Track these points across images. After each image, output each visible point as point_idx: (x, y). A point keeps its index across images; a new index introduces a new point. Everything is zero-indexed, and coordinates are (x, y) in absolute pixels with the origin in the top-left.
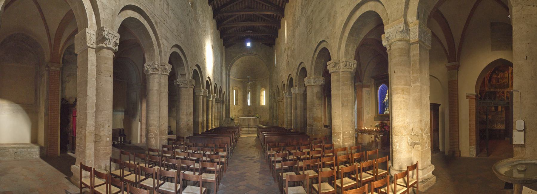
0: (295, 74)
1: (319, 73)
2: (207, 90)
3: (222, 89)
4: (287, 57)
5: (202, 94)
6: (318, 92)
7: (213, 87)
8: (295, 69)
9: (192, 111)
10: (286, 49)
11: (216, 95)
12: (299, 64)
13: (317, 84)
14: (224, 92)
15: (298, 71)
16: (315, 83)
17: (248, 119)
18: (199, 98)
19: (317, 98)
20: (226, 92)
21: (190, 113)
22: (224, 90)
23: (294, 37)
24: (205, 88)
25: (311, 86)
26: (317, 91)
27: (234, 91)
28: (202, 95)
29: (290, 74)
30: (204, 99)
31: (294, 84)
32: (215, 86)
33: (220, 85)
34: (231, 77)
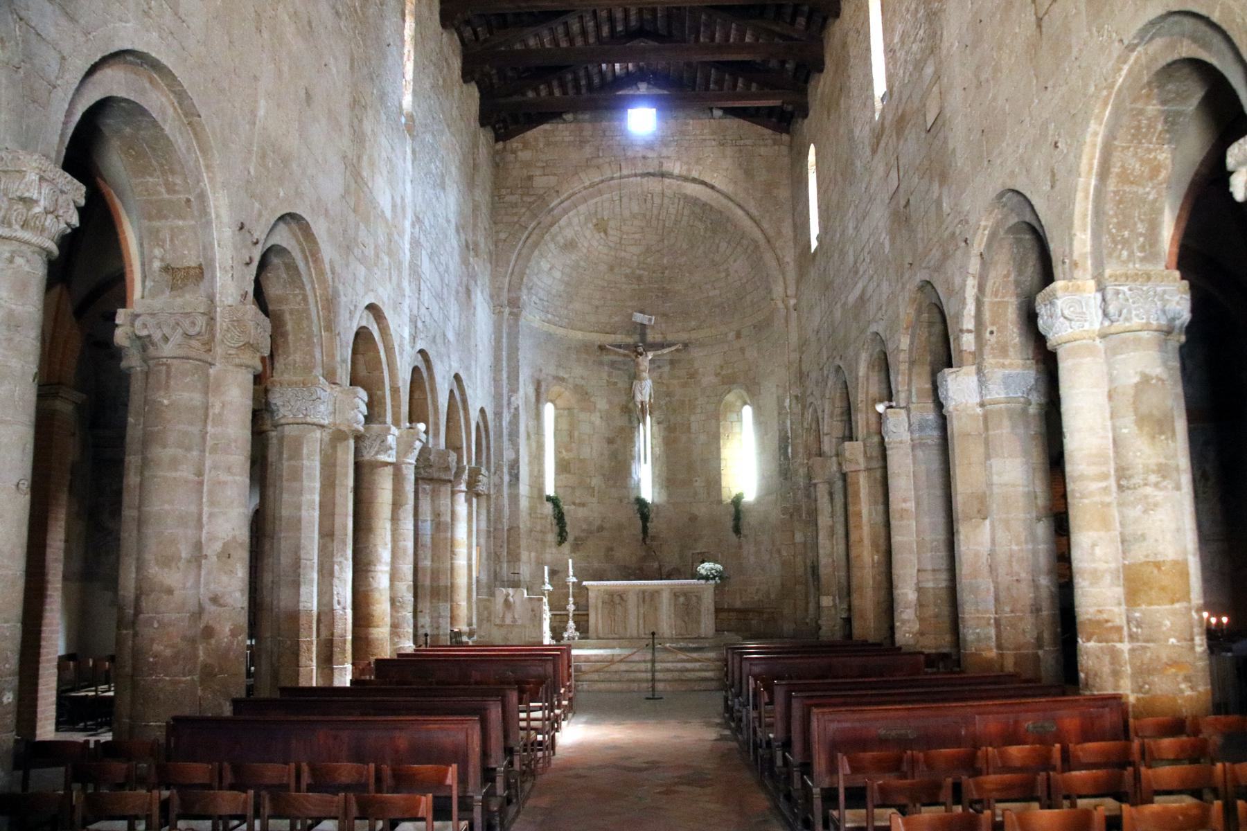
2: (363, 394)
4: (894, 174)
5: (322, 413)
7: (404, 376)
9: (243, 534)
10: (887, 132)
11: (422, 426)
14: (482, 411)
18: (298, 444)
20: (498, 415)
21: (225, 545)
22: (479, 397)
24: (344, 375)
27: (549, 411)
28: (326, 422)
30: (334, 448)
32: (416, 370)
33: (456, 367)
34: (532, 318)
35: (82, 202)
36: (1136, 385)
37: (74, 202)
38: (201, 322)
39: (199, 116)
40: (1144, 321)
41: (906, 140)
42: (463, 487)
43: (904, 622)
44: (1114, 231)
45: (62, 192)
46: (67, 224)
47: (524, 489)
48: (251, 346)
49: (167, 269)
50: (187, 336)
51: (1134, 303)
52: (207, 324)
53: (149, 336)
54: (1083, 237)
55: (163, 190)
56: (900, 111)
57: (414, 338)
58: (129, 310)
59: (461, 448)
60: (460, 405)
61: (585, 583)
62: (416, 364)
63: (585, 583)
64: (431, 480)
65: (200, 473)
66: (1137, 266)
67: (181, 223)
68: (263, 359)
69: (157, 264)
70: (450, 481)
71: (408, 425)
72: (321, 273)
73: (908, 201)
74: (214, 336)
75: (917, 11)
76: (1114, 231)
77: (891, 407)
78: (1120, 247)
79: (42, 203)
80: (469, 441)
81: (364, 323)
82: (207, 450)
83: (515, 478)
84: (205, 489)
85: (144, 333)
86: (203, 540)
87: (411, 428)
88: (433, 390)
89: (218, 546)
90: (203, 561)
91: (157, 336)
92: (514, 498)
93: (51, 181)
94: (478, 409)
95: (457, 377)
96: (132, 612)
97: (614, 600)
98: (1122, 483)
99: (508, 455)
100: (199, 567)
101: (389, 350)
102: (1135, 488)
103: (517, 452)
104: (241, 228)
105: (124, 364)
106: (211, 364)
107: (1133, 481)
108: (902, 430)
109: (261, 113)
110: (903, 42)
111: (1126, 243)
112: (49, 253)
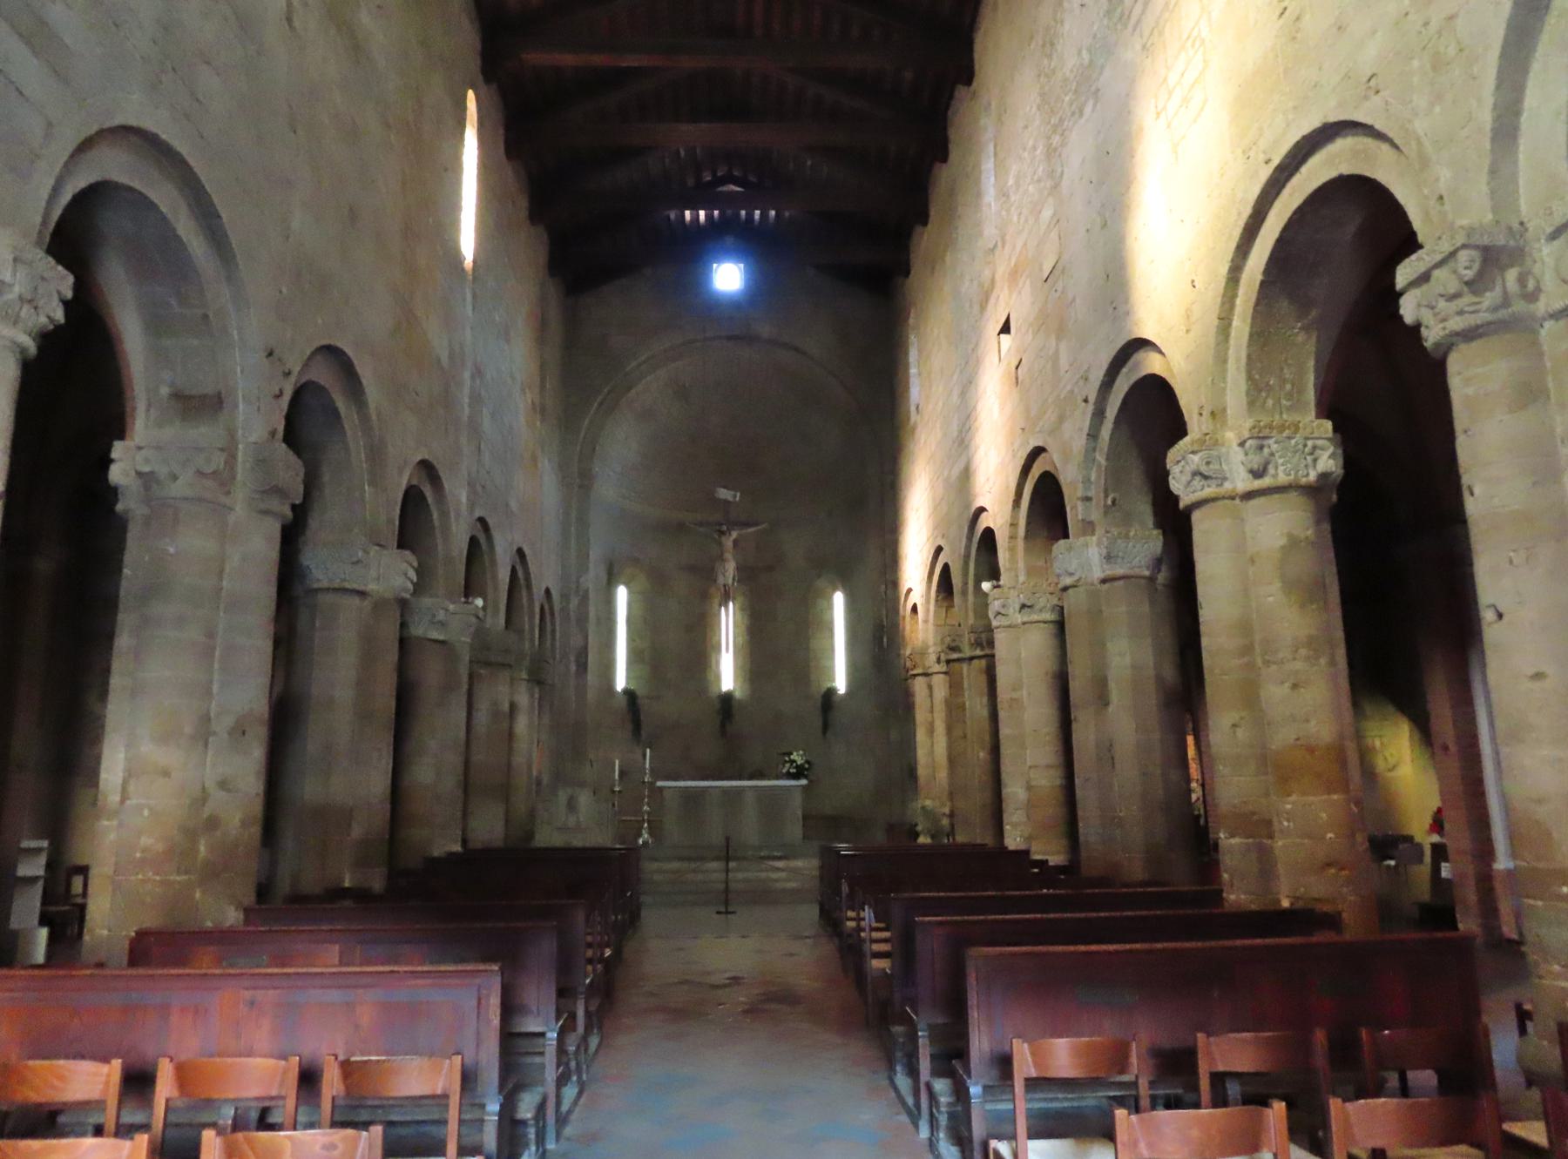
0: (1079, 443)
1: (1289, 396)
3: (532, 568)
6: (1293, 543)
8: (1080, 399)
11: (479, 602)
12: (1105, 366)
13: (1283, 479)
15: (1099, 414)
16: (1258, 474)
17: (725, 791)
19: (1289, 586)
22: (545, 575)
23: (1056, 186)
25: (1233, 498)
26: (1290, 536)
29: (1037, 452)
31: (1075, 512)
33: (518, 539)
35: (69, 294)
36: (1283, 547)
37: (59, 293)
38: (218, 461)
39: (219, 217)
40: (1292, 477)
41: (1020, 293)
42: (524, 676)
43: (1015, 825)
44: (1257, 377)
45: (43, 279)
46: (49, 317)
47: (592, 678)
48: (278, 491)
49: (178, 396)
50: (200, 473)
51: (1280, 457)
52: (226, 463)
53: (152, 473)
54: (1222, 385)
55: (174, 302)
56: (1013, 264)
57: (472, 505)
58: (128, 443)
59: (523, 631)
60: (522, 582)
61: (659, 784)
62: (474, 533)
63: (659, 784)
64: (488, 664)
65: (211, 635)
66: (1285, 416)
67: (196, 342)
68: (294, 507)
69: (165, 391)
70: (510, 666)
71: (463, 599)
72: (365, 418)
73: (1021, 360)
74: (234, 478)
75: (1034, 148)
76: (1257, 377)
77: (998, 586)
78: (1264, 394)
79: (17, 289)
80: (529, 623)
81: (415, 482)
82: (222, 606)
83: (582, 667)
84: (217, 653)
85: (146, 469)
86: (212, 715)
87: (466, 603)
88: (493, 562)
89: (229, 721)
90: (211, 739)
91: (162, 471)
92: (581, 689)
93: (30, 264)
94: (543, 589)
95: (520, 552)
96: (117, 798)
97: (692, 799)
98: (1267, 657)
99: (576, 641)
100: (206, 745)
101: (444, 514)
102: (1282, 663)
103: (586, 638)
104: (270, 354)
105: (119, 507)
106: (231, 509)
107: (1281, 655)
108: (1011, 610)
109: (295, 224)
110: (1017, 184)
111: (1269, 388)
112: (23, 350)
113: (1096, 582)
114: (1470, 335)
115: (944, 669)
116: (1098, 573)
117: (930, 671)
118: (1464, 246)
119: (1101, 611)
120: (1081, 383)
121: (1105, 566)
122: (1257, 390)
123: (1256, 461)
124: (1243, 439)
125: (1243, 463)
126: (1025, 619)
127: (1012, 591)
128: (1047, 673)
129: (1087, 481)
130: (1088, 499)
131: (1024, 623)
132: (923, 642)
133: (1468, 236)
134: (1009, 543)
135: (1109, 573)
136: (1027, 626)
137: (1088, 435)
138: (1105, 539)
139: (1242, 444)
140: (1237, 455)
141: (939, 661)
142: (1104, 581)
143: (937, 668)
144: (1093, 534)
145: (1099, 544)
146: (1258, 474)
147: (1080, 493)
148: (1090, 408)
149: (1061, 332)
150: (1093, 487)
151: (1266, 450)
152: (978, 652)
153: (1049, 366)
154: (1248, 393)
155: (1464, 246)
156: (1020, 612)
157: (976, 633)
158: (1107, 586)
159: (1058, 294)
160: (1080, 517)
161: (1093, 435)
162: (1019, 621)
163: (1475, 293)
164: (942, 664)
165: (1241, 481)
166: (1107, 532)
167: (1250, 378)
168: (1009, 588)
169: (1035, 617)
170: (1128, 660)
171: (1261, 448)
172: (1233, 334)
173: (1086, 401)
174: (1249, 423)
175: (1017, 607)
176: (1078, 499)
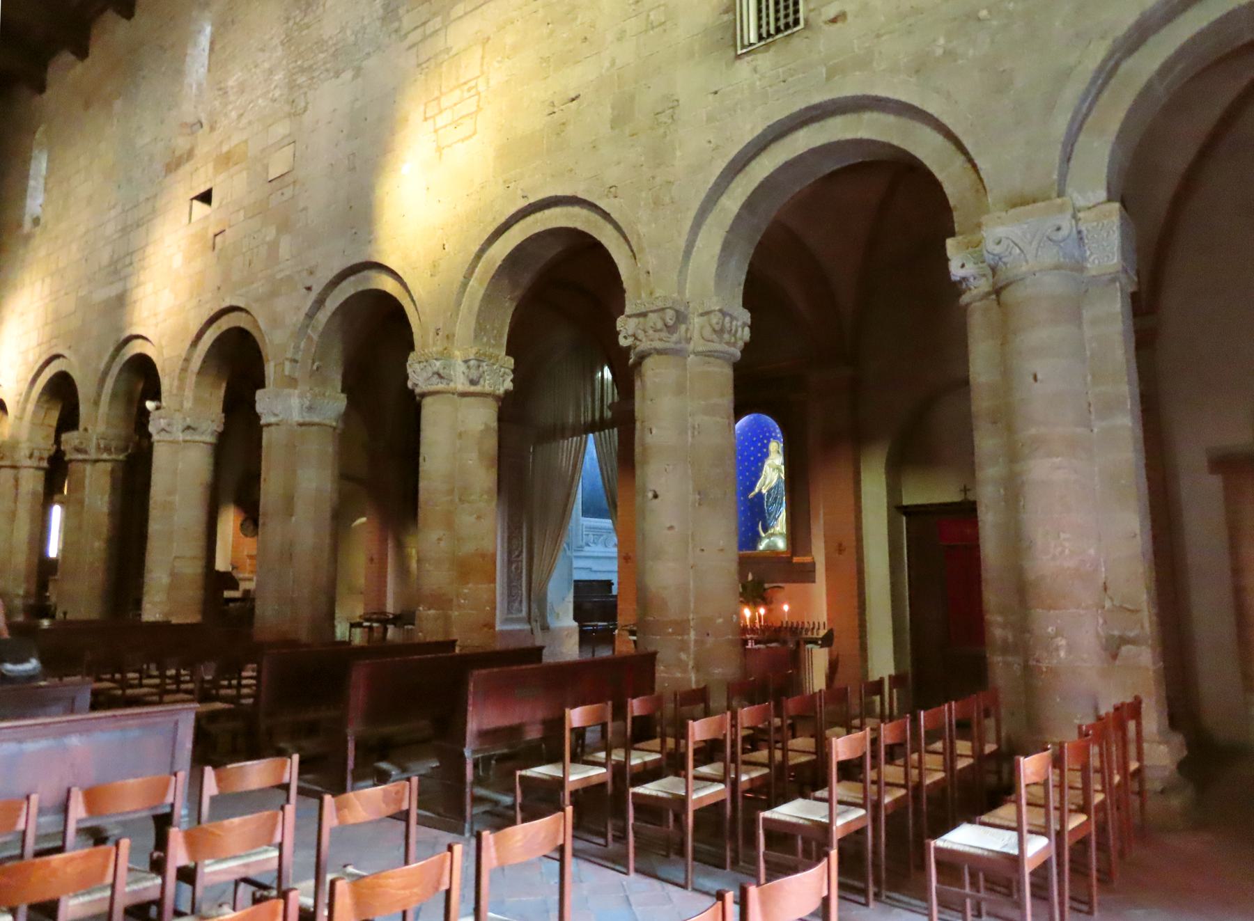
12: (336, 271)
15: (320, 302)
16: (473, 382)
113: (295, 424)
114: (660, 352)
115: (35, 465)
116: (296, 417)
117: (18, 464)
118: (670, 308)
119: (295, 447)
120: (305, 274)
121: (305, 414)
122: (480, 330)
123: (474, 374)
124: (467, 358)
125: (464, 373)
126: (188, 438)
127: (177, 414)
128: (201, 484)
129: (297, 348)
130: (295, 361)
131: (185, 441)
132: (12, 436)
133: (673, 303)
134: (180, 373)
135: (307, 419)
136: (188, 444)
137: (307, 314)
138: (308, 394)
139: (466, 362)
140: (460, 368)
141: (31, 456)
142: (301, 425)
143: (28, 462)
144: (295, 388)
145: (301, 396)
146: (473, 382)
147: (289, 355)
148: (313, 295)
149: (285, 226)
150: (300, 353)
151: (481, 369)
152: (105, 456)
153: (263, 250)
154: (475, 330)
155: (670, 308)
156: (183, 431)
157: (105, 439)
158: (303, 428)
159: (285, 198)
160: (287, 373)
161: (310, 316)
162: (181, 439)
163: (669, 332)
164: (33, 459)
165: (461, 384)
166: (311, 389)
167: (478, 322)
168: (175, 410)
169: (197, 438)
170: (314, 485)
171: (479, 366)
172: (468, 289)
173: (309, 289)
174: (474, 350)
175: (180, 427)
176: (287, 359)
